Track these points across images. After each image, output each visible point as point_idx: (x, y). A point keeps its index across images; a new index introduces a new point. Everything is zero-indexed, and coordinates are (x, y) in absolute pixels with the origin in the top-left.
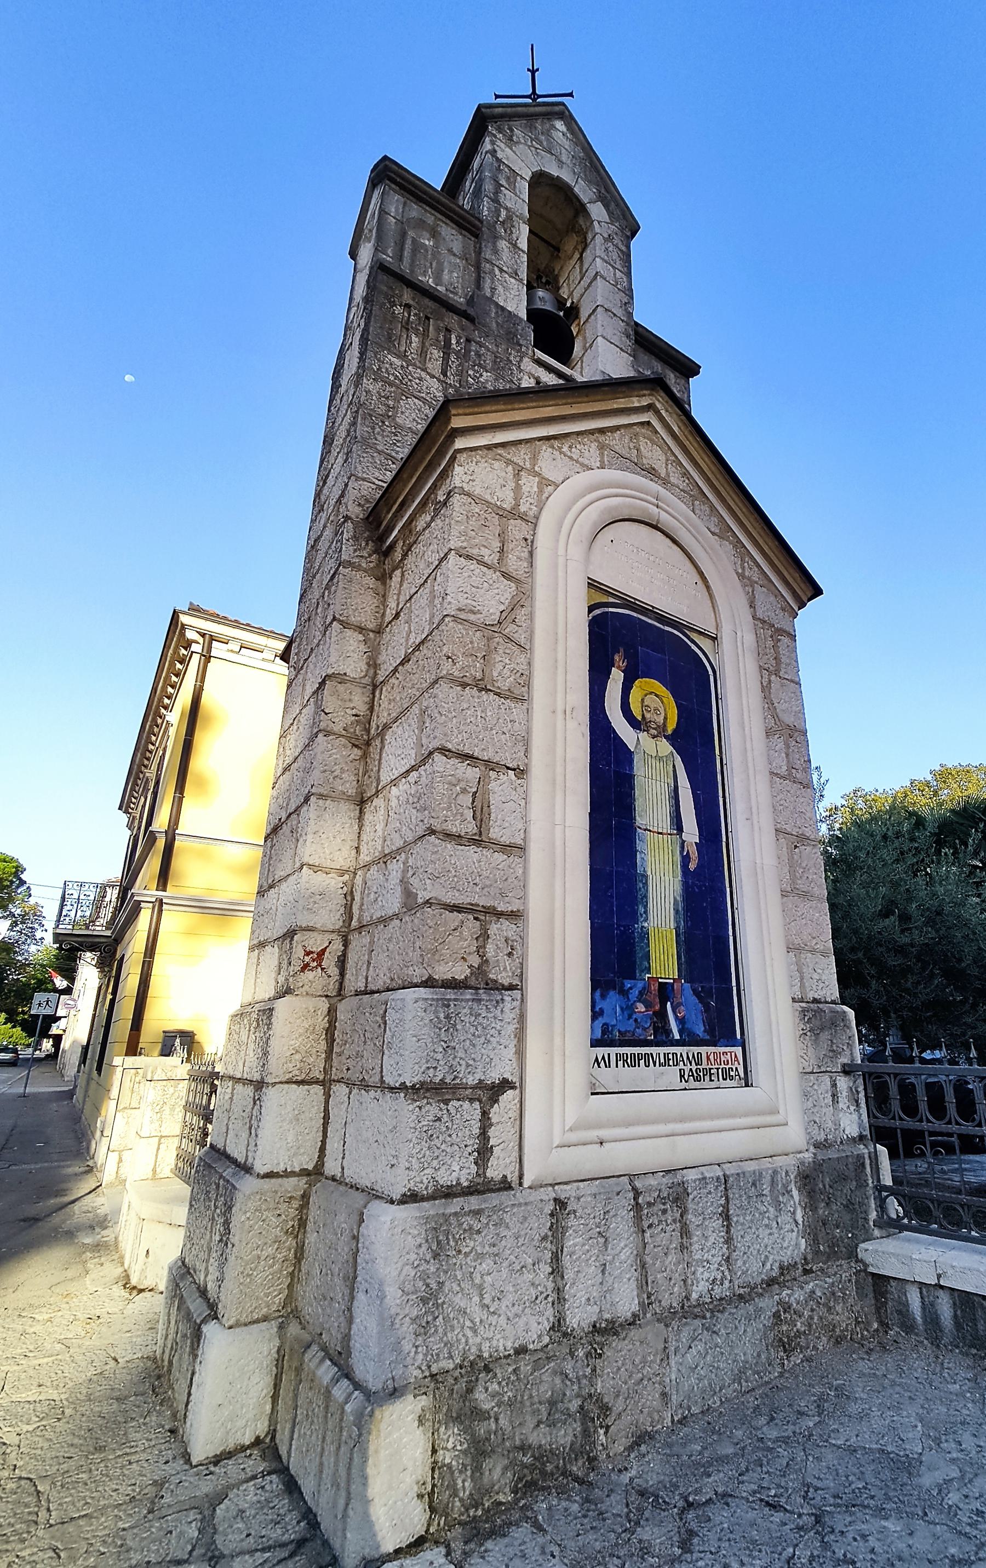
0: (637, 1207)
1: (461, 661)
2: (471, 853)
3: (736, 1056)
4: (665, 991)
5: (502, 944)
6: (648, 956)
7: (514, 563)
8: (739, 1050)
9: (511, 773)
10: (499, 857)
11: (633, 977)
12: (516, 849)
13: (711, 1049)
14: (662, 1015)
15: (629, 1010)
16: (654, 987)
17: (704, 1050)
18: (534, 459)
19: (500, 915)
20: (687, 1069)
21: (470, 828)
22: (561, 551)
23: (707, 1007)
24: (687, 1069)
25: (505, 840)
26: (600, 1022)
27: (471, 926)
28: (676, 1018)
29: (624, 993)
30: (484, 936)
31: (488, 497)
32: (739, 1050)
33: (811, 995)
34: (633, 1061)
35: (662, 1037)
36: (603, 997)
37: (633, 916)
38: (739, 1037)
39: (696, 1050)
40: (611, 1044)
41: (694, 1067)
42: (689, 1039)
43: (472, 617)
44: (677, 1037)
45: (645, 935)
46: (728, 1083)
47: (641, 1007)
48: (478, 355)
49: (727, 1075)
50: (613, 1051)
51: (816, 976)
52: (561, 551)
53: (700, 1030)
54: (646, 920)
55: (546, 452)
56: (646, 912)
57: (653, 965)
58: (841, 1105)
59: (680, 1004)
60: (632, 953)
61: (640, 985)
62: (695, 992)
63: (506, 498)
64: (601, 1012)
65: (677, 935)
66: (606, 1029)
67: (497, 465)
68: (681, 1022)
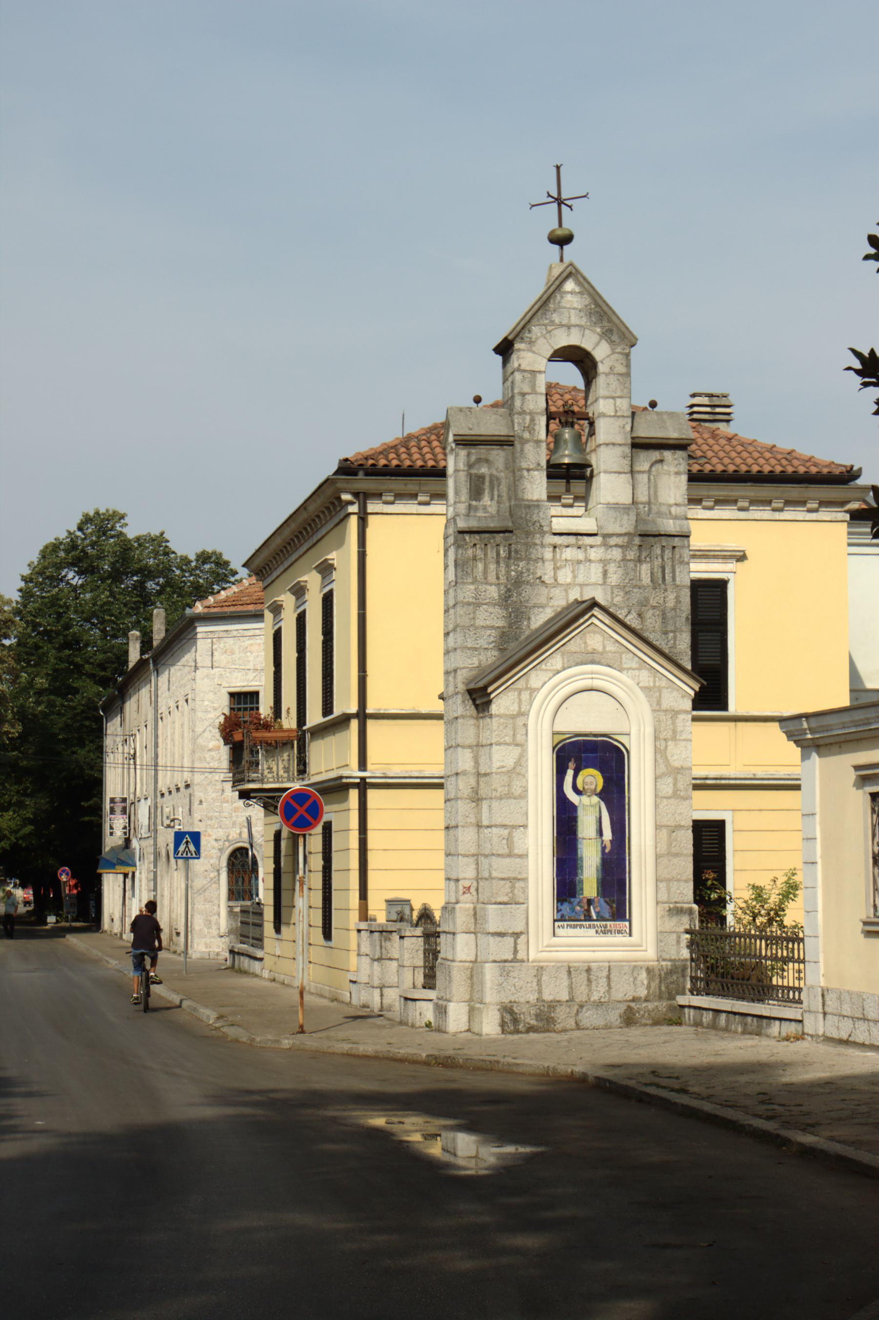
0: (569, 972)
1: (500, 789)
2: (508, 860)
3: (625, 926)
4: (590, 902)
5: (520, 889)
6: (582, 889)
7: (520, 738)
8: (627, 924)
9: (522, 828)
10: (518, 860)
11: (574, 896)
12: (524, 856)
13: (612, 923)
14: (589, 910)
15: (573, 910)
16: (585, 901)
17: (608, 923)
18: (528, 681)
19: (519, 880)
20: (599, 930)
21: (506, 851)
22: (539, 727)
23: (611, 907)
24: (599, 930)
25: (520, 853)
26: (560, 913)
27: (508, 884)
28: (595, 912)
29: (570, 903)
30: (513, 887)
31: (507, 713)
32: (627, 924)
33: (673, 900)
34: (575, 927)
35: (588, 918)
36: (561, 905)
37: (576, 875)
38: (627, 917)
39: (604, 923)
40: (565, 921)
41: (603, 929)
42: (600, 918)
43: (503, 770)
44: (595, 917)
45: (581, 881)
46: (620, 935)
47: (578, 908)
48: (517, 552)
49: (619, 932)
50: (565, 923)
51: (678, 891)
52: (539, 727)
53: (607, 916)
54: (582, 875)
55: (533, 674)
56: (582, 872)
57: (585, 892)
58: (682, 945)
59: (597, 907)
60: (575, 888)
61: (578, 900)
62: (606, 902)
63: (514, 709)
64: (561, 910)
65: (597, 880)
66: (562, 916)
67: (510, 694)
68: (598, 913)
